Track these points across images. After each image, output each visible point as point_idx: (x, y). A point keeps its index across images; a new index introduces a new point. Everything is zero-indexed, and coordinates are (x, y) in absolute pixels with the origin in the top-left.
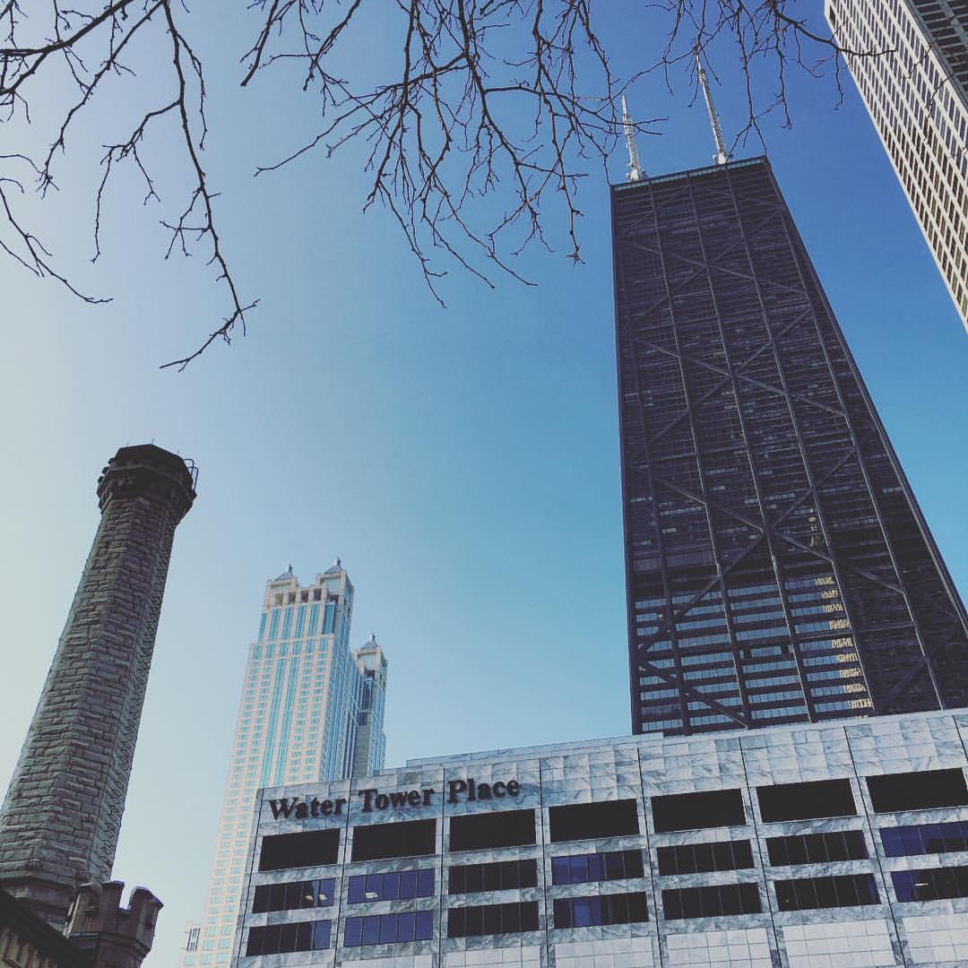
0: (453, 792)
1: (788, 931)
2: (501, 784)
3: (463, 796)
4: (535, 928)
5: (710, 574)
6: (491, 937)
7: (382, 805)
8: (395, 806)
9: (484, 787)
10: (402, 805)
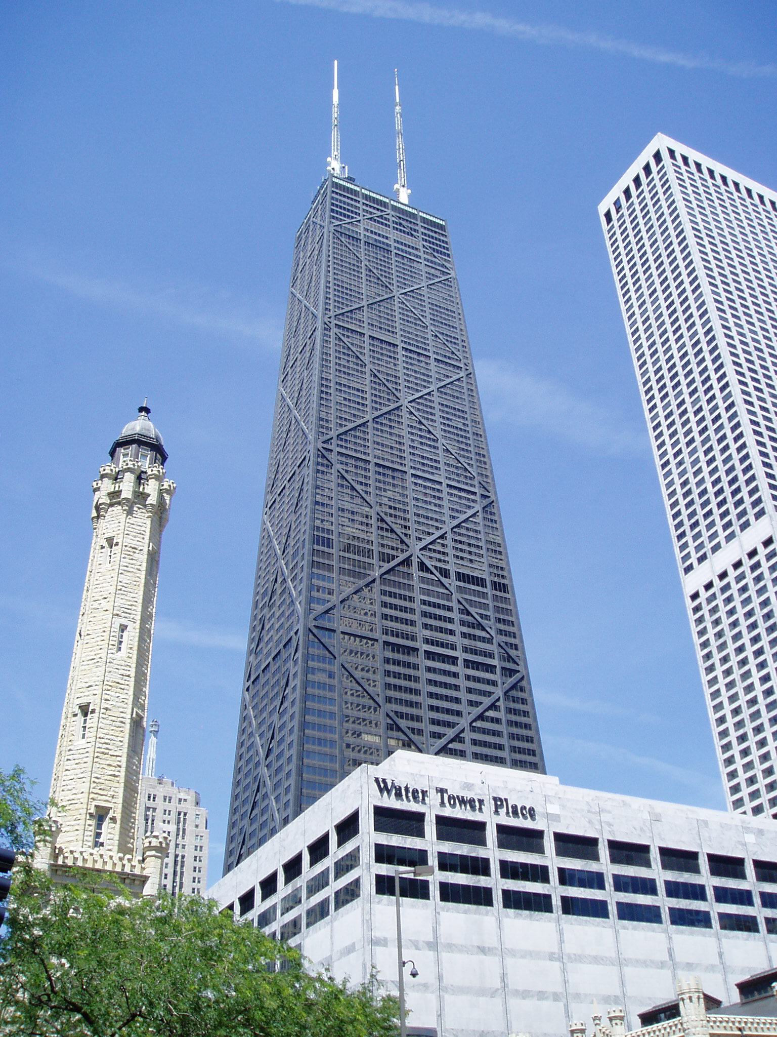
0: (497, 807)
1: (674, 936)
2: (525, 808)
3: (503, 811)
4: (551, 912)
5: (369, 569)
6: (527, 912)
7: (452, 802)
8: (460, 805)
9: (515, 808)
10: (465, 806)
